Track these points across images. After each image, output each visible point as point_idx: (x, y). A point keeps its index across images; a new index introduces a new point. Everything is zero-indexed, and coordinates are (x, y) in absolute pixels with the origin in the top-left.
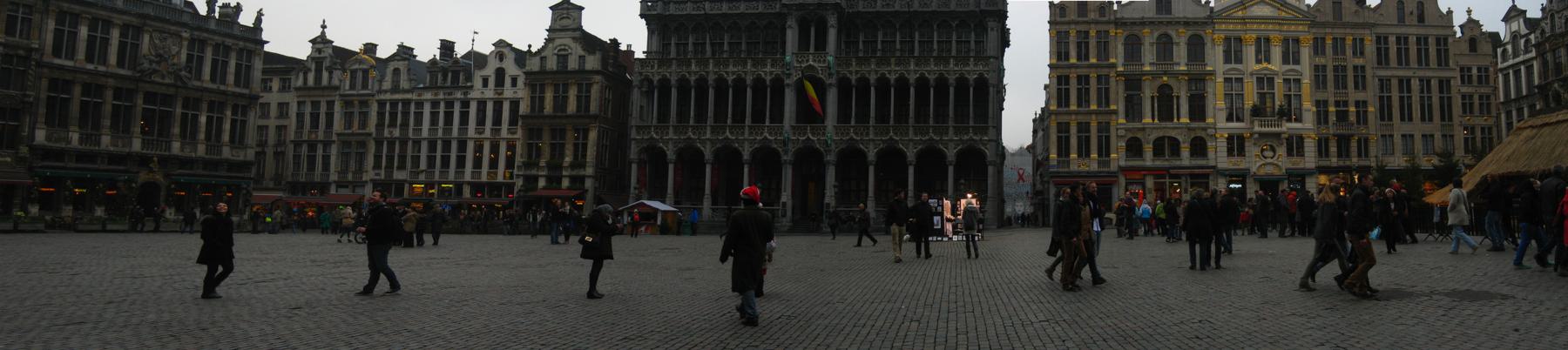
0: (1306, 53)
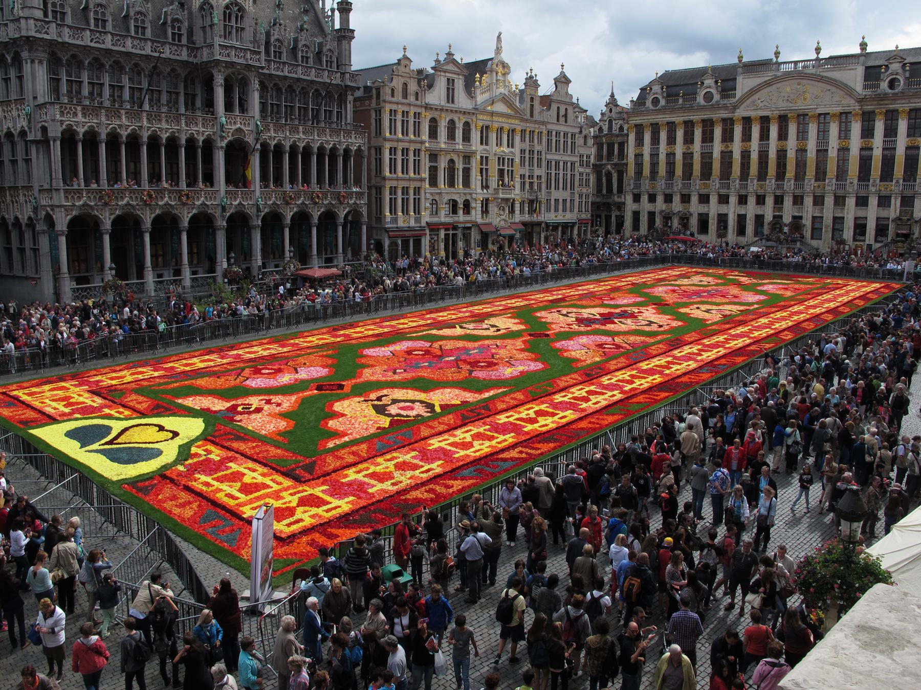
0: (517, 139)
